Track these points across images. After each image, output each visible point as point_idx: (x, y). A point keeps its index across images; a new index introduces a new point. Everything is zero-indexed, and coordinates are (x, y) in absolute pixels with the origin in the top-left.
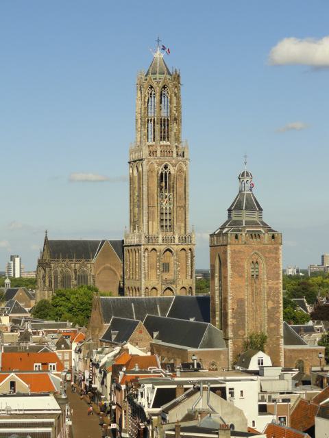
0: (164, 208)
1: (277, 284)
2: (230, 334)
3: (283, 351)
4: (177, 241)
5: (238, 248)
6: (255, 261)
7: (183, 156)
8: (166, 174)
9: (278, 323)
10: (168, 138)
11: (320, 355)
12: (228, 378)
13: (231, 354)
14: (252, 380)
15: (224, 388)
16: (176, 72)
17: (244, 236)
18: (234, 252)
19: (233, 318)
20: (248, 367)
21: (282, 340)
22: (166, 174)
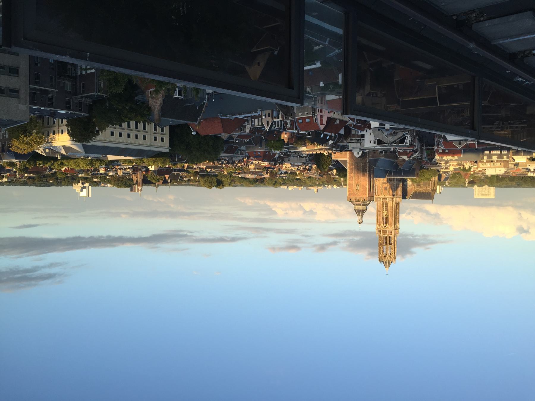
0: (386, 211)
1: (349, 182)
2: (368, 164)
3: (348, 158)
4: (381, 199)
5: (364, 196)
6: (358, 190)
7: (378, 230)
8: (385, 224)
9: (349, 168)
10: (384, 238)
11: (334, 156)
12: (374, 148)
13: (368, 157)
14: (367, 147)
15: (378, 144)
16: (380, 262)
17: (362, 200)
18: (366, 194)
19: (366, 170)
20: (363, 151)
21: (348, 162)
22: (385, 224)
